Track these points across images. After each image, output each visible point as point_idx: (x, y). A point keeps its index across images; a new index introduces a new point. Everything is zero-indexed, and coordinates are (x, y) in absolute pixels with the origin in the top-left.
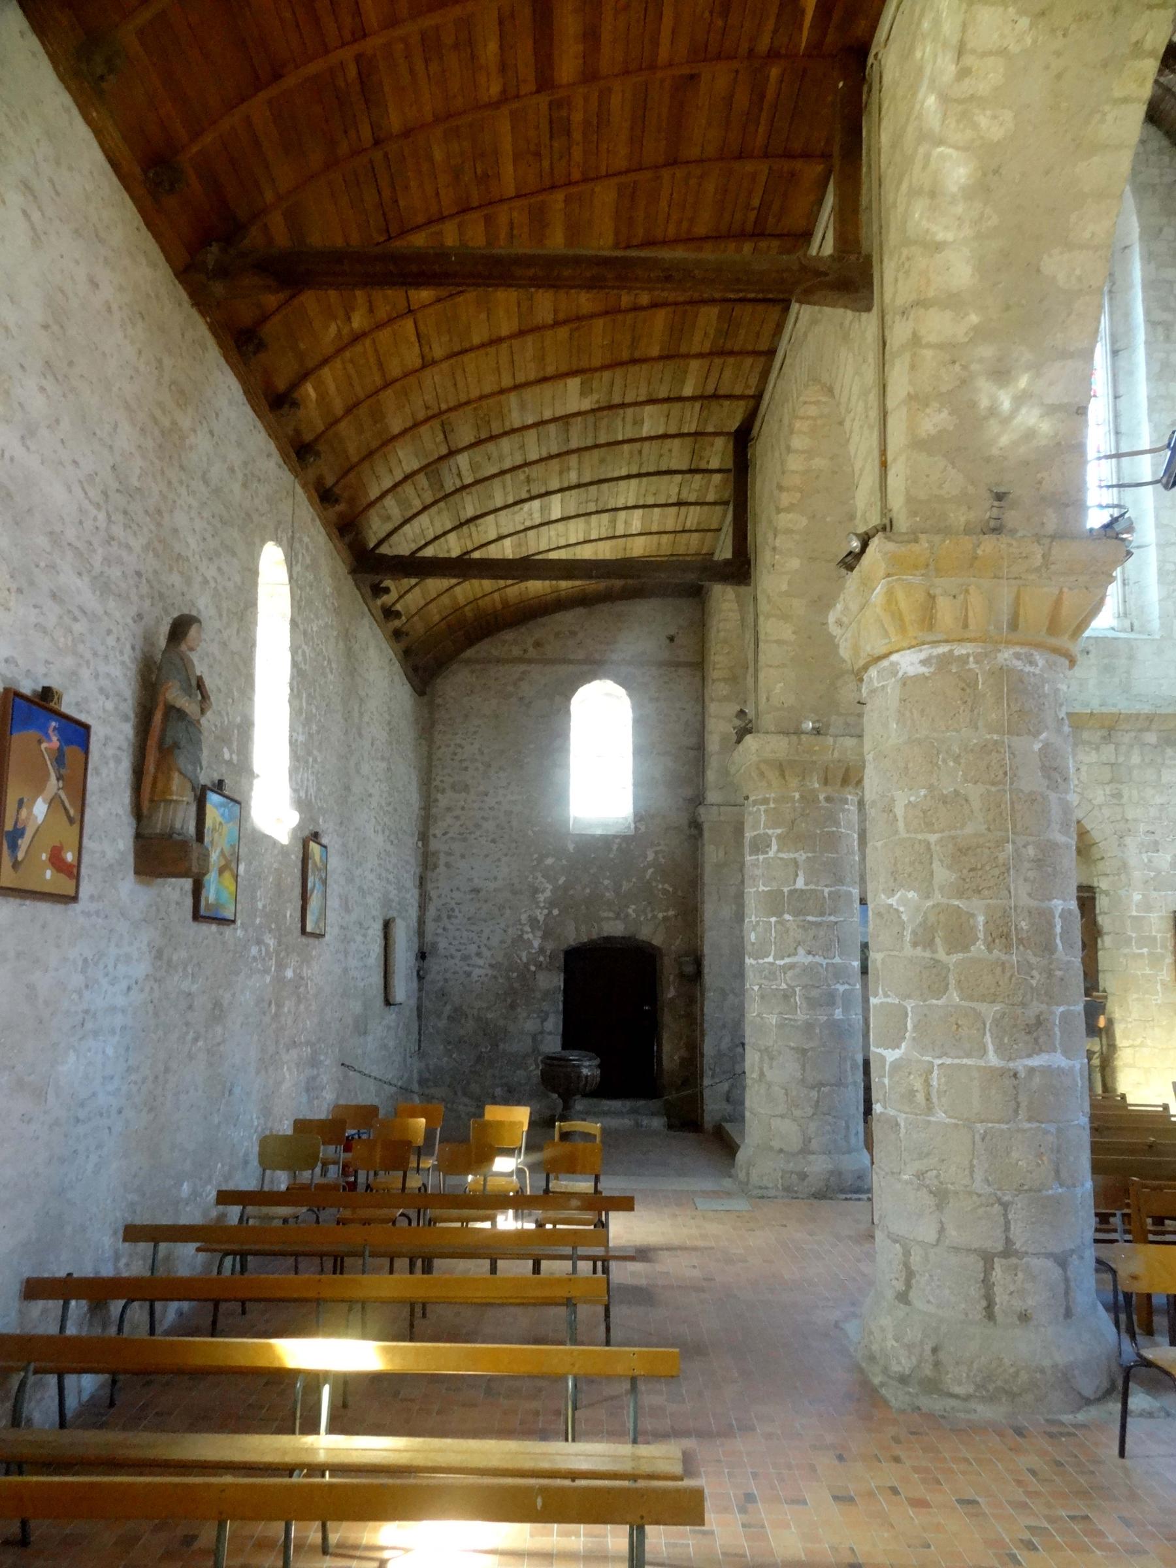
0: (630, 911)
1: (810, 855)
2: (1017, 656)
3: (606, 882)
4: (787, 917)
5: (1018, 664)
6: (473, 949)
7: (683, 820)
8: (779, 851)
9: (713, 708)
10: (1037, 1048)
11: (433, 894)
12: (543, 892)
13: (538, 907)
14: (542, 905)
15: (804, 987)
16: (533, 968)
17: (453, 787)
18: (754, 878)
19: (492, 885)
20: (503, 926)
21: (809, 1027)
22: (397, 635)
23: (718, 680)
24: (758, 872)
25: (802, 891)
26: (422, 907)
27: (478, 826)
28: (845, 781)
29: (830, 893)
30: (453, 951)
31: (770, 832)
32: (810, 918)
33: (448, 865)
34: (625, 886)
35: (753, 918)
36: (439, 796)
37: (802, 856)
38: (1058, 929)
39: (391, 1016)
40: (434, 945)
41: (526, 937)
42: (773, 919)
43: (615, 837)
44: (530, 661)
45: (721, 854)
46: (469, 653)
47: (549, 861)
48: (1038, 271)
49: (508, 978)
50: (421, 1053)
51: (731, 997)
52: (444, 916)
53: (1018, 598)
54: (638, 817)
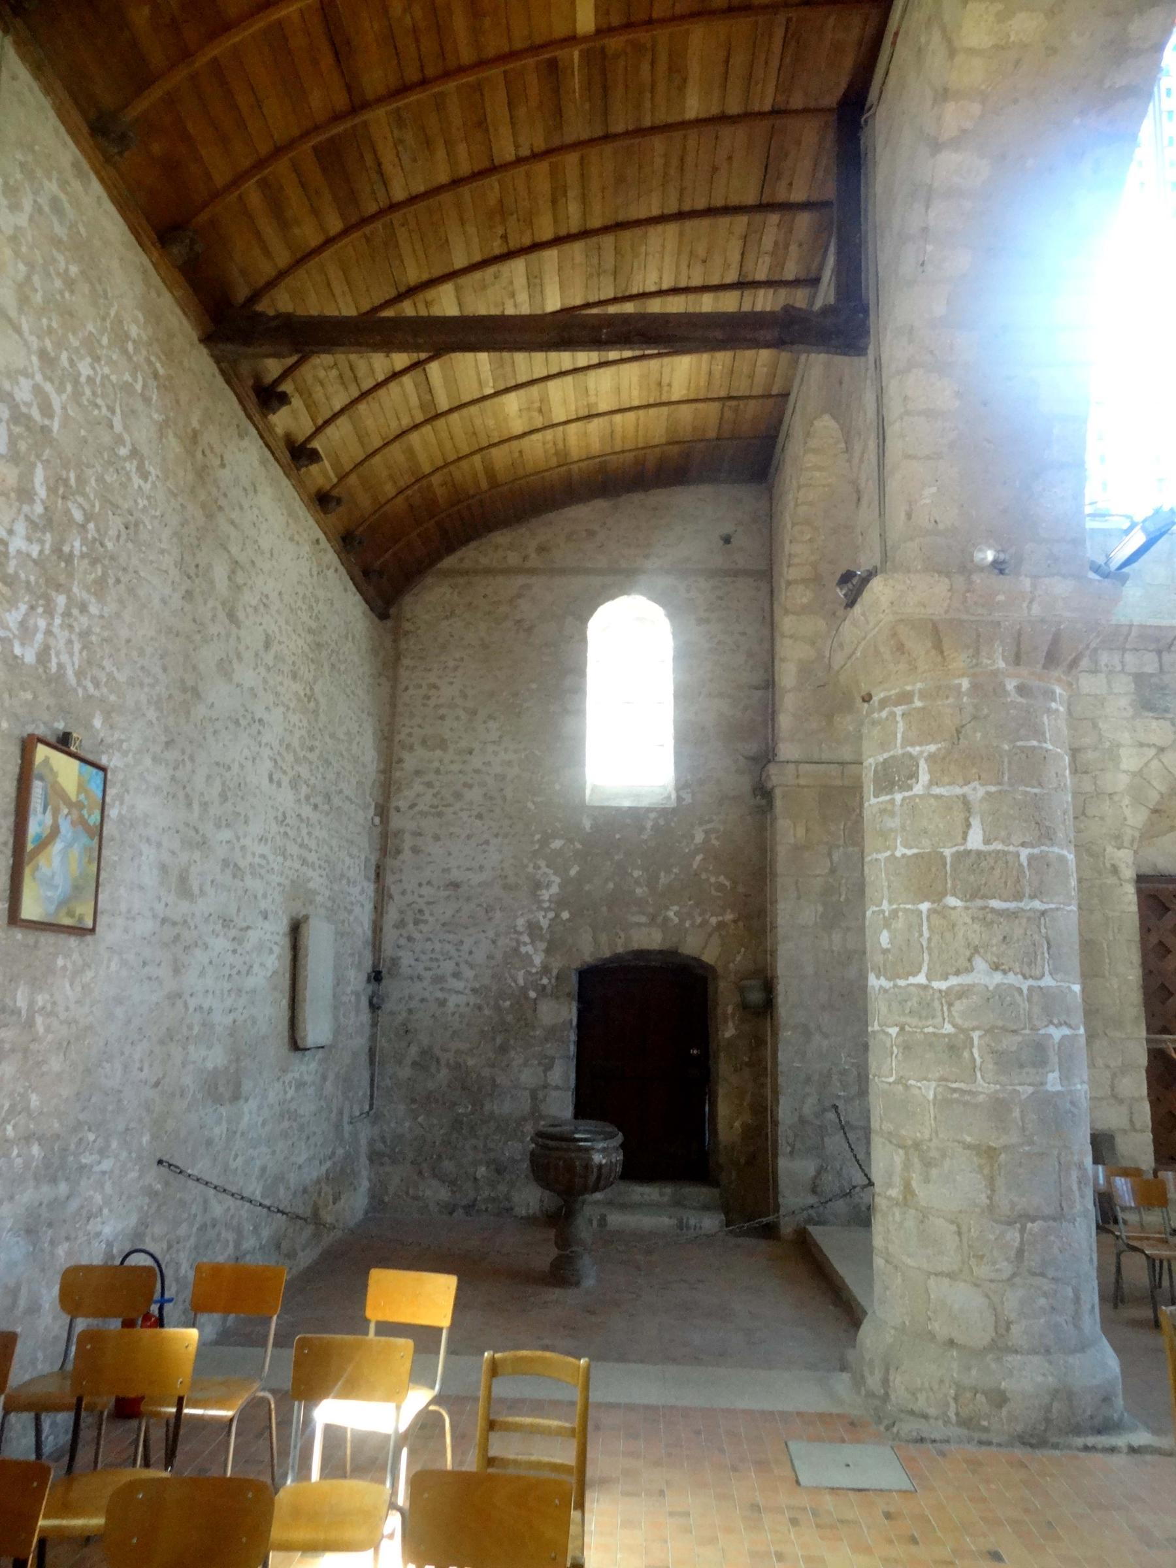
0: (671, 914)
1: (993, 789)
3: (637, 873)
4: (952, 901)
6: (448, 967)
7: (744, 784)
8: (933, 782)
9: (787, 623)
11: (394, 890)
12: (548, 886)
13: (540, 908)
14: (546, 905)
15: (989, 1031)
16: (532, 994)
17: (424, 742)
18: (884, 834)
19: (476, 878)
20: (491, 934)
21: (999, 1108)
22: (323, 501)
23: (796, 582)
24: (893, 823)
25: (979, 853)
26: (379, 909)
28: (1051, 659)
29: (1031, 858)
30: (420, 968)
31: (915, 750)
32: (995, 904)
33: (415, 850)
34: (663, 879)
35: (885, 905)
36: (405, 755)
37: (977, 792)
39: (306, 1068)
40: (395, 961)
41: (523, 950)
42: (925, 907)
43: (649, 810)
44: (532, 571)
45: (801, 832)
46: (449, 562)
47: (557, 844)
49: (498, 1009)
50: (373, 1115)
51: (817, 1037)
52: (409, 918)
54: (681, 786)
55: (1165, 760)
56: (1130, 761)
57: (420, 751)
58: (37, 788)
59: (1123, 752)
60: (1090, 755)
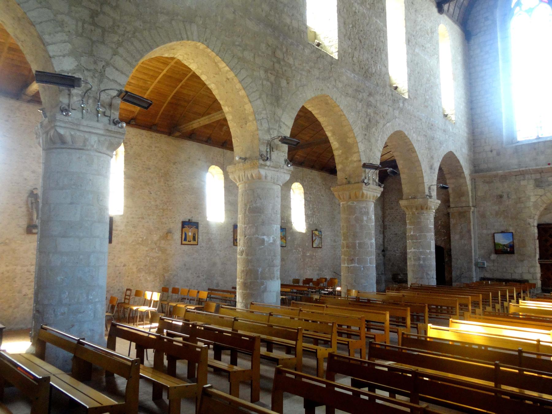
2: (351, 203)
4: (410, 241)
5: (351, 204)
6: (396, 249)
10: (352, 263)
15: (413, 256)
21: (414, 265)
26: (384, 239)
27: (396, 218)
28: (422, 209)
32: (414, 241)
33: (389, 228)
36: (386, 211)
37: (412, 227)
38: (357, 245)
40: (387, 248)
48: (347, 142)
53: (350, 194)
55: (542, 198)
56: (533, 199)
57: (389, 210)
58: (314, 235)
59: (531, 197)
60: (523, 199)
